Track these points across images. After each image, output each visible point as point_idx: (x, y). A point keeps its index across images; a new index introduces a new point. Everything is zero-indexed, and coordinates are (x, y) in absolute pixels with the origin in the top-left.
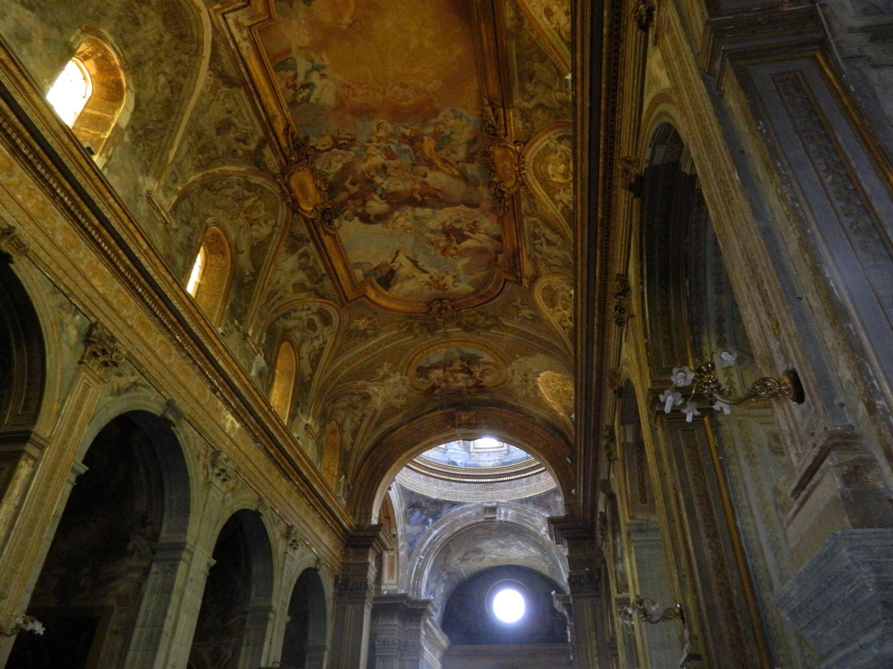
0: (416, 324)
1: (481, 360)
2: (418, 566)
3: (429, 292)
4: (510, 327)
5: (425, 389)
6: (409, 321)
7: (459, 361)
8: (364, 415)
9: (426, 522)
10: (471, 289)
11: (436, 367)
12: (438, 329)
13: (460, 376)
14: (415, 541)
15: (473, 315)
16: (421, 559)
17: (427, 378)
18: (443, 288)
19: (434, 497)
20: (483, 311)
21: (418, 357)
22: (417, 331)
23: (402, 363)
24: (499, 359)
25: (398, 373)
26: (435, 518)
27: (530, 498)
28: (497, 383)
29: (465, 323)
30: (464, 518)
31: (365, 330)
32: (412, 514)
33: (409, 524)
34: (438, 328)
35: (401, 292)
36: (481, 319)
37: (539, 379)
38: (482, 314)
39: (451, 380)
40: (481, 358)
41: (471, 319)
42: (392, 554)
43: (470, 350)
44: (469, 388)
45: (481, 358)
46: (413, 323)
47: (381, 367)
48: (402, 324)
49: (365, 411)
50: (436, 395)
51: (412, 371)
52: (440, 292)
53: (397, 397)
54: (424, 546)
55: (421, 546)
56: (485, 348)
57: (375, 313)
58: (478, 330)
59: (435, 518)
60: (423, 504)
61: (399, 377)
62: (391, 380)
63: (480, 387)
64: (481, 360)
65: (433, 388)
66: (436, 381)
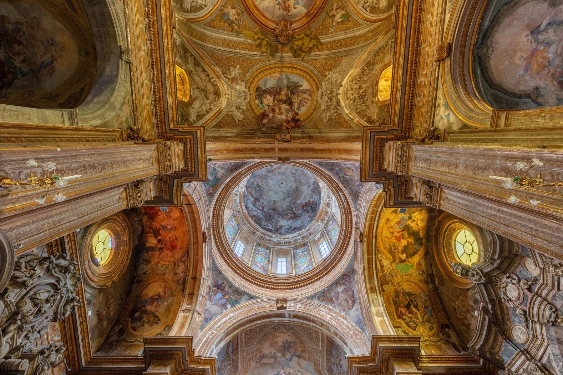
0: (265, 42)
1: (301, 88)
2: (208, 338)
3: (279, 12)
4: (325, 43)
5: (258, 113)
6: (262, 37)
7: (285, 89)
8: (210, 109)
9: (224, 306)
10: (304, 11)
11: (268, 92)
12: (278, 52)
13: (284, 107)
14: (211, 319)
15: (302, 39)
16: (212, 333)
17: (262, 102)
18: (287, 9)
19: (237, 286)
20: (308, 32)
21: (259, 76)
22: (264, 49)
23: (248, 75)
24: (313, 83)
25: (243, 83)
26: (233, 305)
27: (315, 294)
28: (309, 114)
29: (295, 47)
30: (259, 308)
31: (233, 22)
32: (215, 293)
33: (211, 301)
34: (277, 51)
35: (261, 4)
36: (307, 40)
37: (341, 91)
38: (308, 36)
39: (277, 111)
40: (301, 86)
41: (300, 43)
42: (187, 314)
43: (295, 79)
44: (288, 122)
45: (301, 86)
46: (263, 40)
47: (235, 68)
48: (256, 37)
49: (212, 106)
50: (264, 126)
51: (253, 89)
52: (285, 13)
53: (238, 108)
54: (219, 324)
55: (215, 323)
56: (305, 75)
57: (242, 12)
58: (303, 54)
59: (233, 305)
60: (227, 289)
61: (243, 89)
62: (238, 87)
63: (295, 123)
64: (301, 88)
65: (264, 115)
66: (266, 108)
